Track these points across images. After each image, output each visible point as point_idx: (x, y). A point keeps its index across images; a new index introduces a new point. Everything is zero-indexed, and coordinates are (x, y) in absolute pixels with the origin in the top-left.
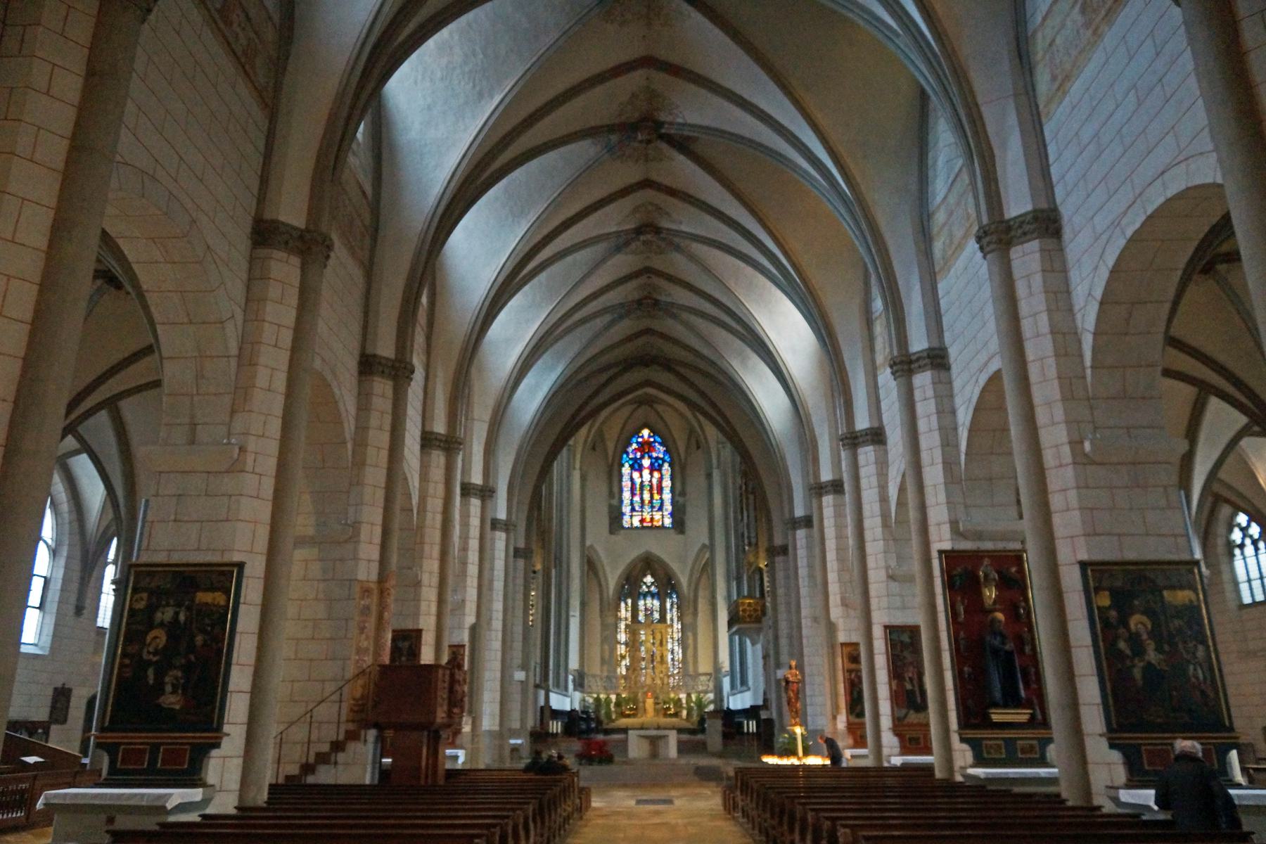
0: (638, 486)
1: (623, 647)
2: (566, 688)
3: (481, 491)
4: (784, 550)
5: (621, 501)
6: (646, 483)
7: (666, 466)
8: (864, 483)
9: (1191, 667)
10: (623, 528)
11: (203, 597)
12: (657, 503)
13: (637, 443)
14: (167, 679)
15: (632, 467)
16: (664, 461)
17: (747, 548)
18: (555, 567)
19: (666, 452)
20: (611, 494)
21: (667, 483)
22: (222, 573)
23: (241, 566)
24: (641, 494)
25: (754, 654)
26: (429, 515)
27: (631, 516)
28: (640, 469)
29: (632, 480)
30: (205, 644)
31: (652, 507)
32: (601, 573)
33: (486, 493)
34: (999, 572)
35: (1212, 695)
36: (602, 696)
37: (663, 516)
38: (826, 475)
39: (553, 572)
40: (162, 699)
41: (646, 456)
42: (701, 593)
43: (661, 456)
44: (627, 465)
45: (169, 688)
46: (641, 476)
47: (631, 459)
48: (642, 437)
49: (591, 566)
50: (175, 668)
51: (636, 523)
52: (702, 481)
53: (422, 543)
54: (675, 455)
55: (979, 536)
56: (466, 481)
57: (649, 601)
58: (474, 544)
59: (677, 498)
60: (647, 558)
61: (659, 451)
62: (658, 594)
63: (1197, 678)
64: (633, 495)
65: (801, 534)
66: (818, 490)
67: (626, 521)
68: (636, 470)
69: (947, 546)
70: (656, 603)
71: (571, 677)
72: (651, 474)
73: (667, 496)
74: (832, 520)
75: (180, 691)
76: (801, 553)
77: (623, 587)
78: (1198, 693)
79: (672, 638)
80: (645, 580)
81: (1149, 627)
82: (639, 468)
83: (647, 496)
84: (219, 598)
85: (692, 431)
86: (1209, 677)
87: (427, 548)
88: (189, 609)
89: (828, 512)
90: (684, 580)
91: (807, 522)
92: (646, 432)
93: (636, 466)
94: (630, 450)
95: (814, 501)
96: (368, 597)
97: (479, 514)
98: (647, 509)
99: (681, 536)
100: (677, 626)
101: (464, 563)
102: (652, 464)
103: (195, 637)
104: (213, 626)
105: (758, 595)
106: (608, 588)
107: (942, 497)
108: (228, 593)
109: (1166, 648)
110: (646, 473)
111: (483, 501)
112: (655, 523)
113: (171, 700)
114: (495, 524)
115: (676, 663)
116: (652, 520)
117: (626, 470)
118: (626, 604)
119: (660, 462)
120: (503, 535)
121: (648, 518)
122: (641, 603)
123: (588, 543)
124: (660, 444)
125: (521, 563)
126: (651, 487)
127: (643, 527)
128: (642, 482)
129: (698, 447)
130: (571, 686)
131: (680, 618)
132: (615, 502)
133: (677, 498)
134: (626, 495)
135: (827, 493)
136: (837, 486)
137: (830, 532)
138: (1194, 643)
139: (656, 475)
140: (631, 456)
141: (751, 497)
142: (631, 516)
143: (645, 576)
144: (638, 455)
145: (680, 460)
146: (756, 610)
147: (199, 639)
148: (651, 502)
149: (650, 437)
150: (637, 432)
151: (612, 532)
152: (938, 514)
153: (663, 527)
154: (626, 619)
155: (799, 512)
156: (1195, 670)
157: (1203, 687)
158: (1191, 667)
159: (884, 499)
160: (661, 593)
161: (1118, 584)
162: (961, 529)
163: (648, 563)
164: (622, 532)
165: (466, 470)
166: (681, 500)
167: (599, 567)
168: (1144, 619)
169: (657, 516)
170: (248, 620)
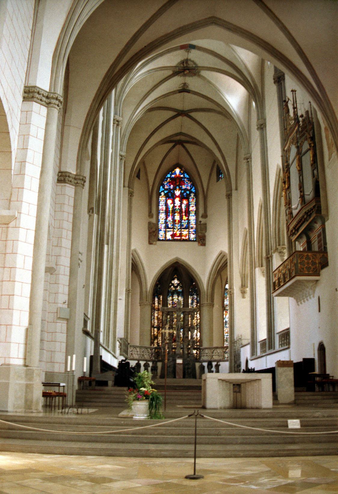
2: (114, 351)
5: (158, 221)
6: (177, 208)
7: (192, 195)
10: (159, 240)
15: (167, 196)
16: (191, 192)
18: (108, 244)
19: (193, 185)
20: (150, 215)
21: (192, 208)
24: (173, 216)
27: (165, 232)
28: (173, 197)
29: (166, 205)
31: (182, 225)
37: (189, 231)
39: (106, 247)
41: (178, 188)
43: (189, 188)
44: (163, 194)
46: (173, 203)
48: (175, 173)
51: (169, 237)
52: (225, 201)
57: (175, 297)
59: (200, 219)
62: (183, 291)
68: (169, 198)
70: (181, 299)
71: (118, 344)
73: (192, 218)
80: (173, 282)
82: (173, 197)
83: (177, 217)
92: (178, 171)
98: (178, 226)
99: (202, 247)
106: (146, 283)
110: (177, 201)
112: (183, 237)
116: (181, 235)
117: (162, 199)
118: (159, 299)
119: (188, 192)
120: (44, 110)
121: (178, 233)
122: (170, 298)
123: (133, 248)
124: (190, 180)
125: (70, 190)
128: (174, 207)
132: (154, 220)
133: (200, 219)
134: (162, 216)
139: (185, 202)
143: (174, 279)
145: (203, 191)
146: (314, 263)
148: (180, 221)
150: (171, 170)
151: (150, 243)
153: (189, 240)
164: (158, 242)
166: (203, 220)
167: (140, 266)
169: (185, 232)
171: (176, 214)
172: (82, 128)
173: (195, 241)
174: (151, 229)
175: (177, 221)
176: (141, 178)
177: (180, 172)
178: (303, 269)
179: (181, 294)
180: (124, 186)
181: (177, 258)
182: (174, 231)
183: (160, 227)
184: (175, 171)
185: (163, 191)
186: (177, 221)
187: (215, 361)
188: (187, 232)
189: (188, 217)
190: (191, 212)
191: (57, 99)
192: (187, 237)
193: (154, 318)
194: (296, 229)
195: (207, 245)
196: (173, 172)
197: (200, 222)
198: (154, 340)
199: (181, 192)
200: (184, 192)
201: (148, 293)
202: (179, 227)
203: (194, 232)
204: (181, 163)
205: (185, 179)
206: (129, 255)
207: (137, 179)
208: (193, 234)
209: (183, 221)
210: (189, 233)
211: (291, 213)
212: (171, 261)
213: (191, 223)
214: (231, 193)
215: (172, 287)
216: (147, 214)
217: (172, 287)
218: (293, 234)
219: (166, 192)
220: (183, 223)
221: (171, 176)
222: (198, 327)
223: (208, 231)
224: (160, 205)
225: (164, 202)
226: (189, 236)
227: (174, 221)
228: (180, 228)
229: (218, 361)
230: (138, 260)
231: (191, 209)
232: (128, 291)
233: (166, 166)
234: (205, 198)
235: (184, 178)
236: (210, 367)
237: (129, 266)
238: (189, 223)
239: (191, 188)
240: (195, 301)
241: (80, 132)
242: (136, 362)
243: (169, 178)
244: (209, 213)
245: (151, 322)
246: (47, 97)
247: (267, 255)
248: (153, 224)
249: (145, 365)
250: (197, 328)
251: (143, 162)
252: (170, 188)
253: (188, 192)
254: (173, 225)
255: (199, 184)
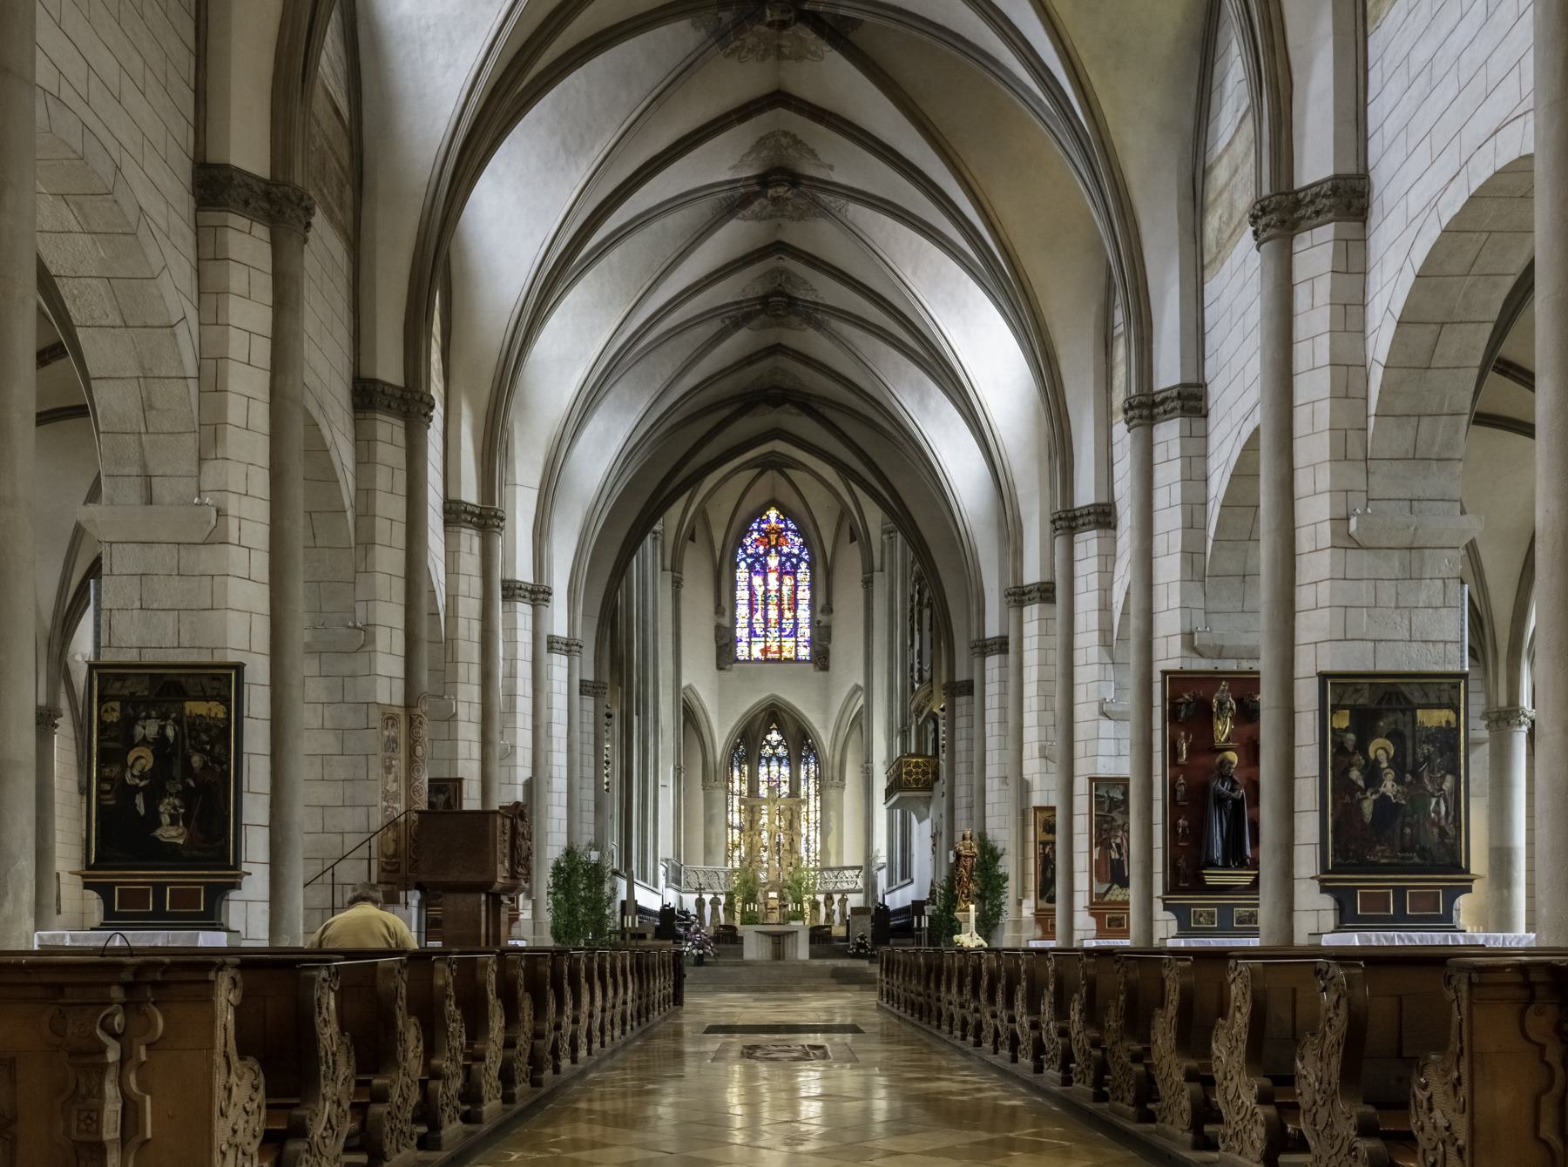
0: (759, 598)
1: (736, 832)
2: (656, 884)
3: (532, 592)
4: (968, 688)
5: (734, 620)
6: (773, 594)
7: (803, 565)
8: (1080, 585)
9: (1434, 801)
10: (737, 660)
11: (195, 708)
12: (788, 627)
13: (759, 530)
14: (162, 809)
15: (751, 567)
16: (800, 560)
17: (917, 686)
18: (638, 714)
19: (804, 544)
20: (719, 610)
21: (804, 595)
22: (215, 678)
23: (239, 668)
24: (766, 610)
25: (921, 833)
26: (462, 623)
27: (750, 643)
29: (751, 587)
30: (205, 766)
31: (782, 630)
32: (705, 730)
33: (538, 595)
34: (1239, 701)
35: (1452, 833)
36: (707, 898)
37: (797, 642)
38: (1032, 574)
39: (635, 718)
40: (158, 832)
41: (773, 550)
42: (850, 757)
43: (796, 551)
44: (743, 565)
45: (166, 819)
47: (751, 556)
48: (768, 521)
49: (690, 717)
50: (171, 795)
53: (455, 662)
54: (818, 552)
55: (1220, 653)
56: (508, 577)
58: (524, 669)
59: (819, 617)
60: (773, 705)
61: (793, 544)
63: (1438, 813)
64: (752, 610)
65: (993, 662)
66: (1018, 596)
67: (742, 650)
68: (757, 573)
69: (1174, 665)
70: (785, 771)
71: (661, 870)
72: (780, 580)
73: (804, 614)
74: (1035, 640)
75: (181, 823)
76: (992, 689)
77: (736, 748)
78: (1436, 830)
79: (807, 820)
81: (1392, 752)
83: (773, 614)
84: (217, 710)
85: (844, 513)
86: (1452, 813)
87: (462, 668)
88: (178, 722)
89: (1031, 628)
90: (824, 735)
91: (1002, 645)
92: (773, 514)
93: (758, 567)
94: (748, 541)
95: (1013, 613)
96: (393, 725)
97: (529, 626)
98: (773, 632)
99: (821, 674)
100: (814, 804)
101: (511, 696)
102: (781, 564)
103: (191, 757)
104: (212, 743)
105: (930, 753)
106: (713, 747)
107: (1176, 601)
108: (225, 701)
109: (1408, 777)
110: (772, 577)
111: (533, 606)
112: (786, 654)
113: (170, 833)
114: (553, 645)
115: (812, 855)
117: (742, 574)
118: (741, 771)
119: (794, 560)
120: (565, 659)
122: (763, 771)
123: (684, 683)
126: (780, 599)
127: (767, 660)
128: (766, 591)
129: (853, 539)
130: (662, 881)
131: (820, 792)
132: (726, 622)
133: (819, 617)
134: (742, 611)
135: (1031, 601)
136: (1046, 590)
137: (1031, 657)
138: (1443, 772)
139: (788, 580)
140: (749, 552)
141: (927, 613)
142: (750, 643)
144: (761, 550)
146: (925, 773)
147: (196, 760)
149: (779, 521)
150: (760, 512)
151: (720, 667)
152: (1169, 624)
153: (797, 660)
154: (741, 793)
155: (992, 630)
156: (1438, 803)
157: (1443, 823)
158: (1434, 801)
159: (1105, 607)
160: (793, 755)
161: (1361, 701)
162: (1196, 643)
163: (774, 714)
165: (510, 560)
168: (1388, 742)
169: (789, 644)
170: (256, 738)
171: (770, 607)
172: (598, 615)
173: (810, 661)
174: (722, 639)
175: (773, 621)
176: (697, 538)
177: (778, 517)
178: (909, 781)
179: (785, 761)
180: (663, 569)
181: (773, 695)
182: (766, 642)
183: (738, 635)
184: (768, 516)
185: (744, 559)
186: (773, 621)
187: (837, 892)
188: (794, 644)
189: (795, 611)
190: (800, 602)
191: (577, 645)
192: (793, 654)
193: (732, 811)
194: (919, 712)
195: (831, 668)
196: (764, 517)
197: (819, 622)
198: (733, 851)
199: (780, 560)
200: (786, 561)
201: (718, 766)
202: (777, 634)
203: (806, 644)
204: (781, 499)
205: (789, 533)
206: (678, 702)
207: (690, 542)
208: (805, 647)
209: (784, 621)
210: (797, 646)
211: (913, 686)
212: (761, 702)
213: (800, 625)
214: (872, 577)
215: (767, 747)
216: (713, 610)
217: (767, 747)
218: (918, 717)
219: (749, 561)
220: (784, 626)
221: (759, 526)
222: (818, 825)
223: (833, 642)
224: (739, 588)
225: (746, 583)
226: (796, 650)
227: (766, 620)
228: (780, 636)
229: (844, 893)
230: (696, 703)
231: (800, 595)
232: (678, 771)
233: (749, 505)
234: (829, 573)
235: (787, 529)
236: (829, 903)
237: (678, 711)
238: (796, 624)
239: (801, 552)
240: (813, 775)
241: (596, 621)
242: (697, 896)
243: (756, 530)
244: (835, 608)
245: (727, 819)
246: (567, 645)
247: (903, 727)
248: (725, 628)
249: (712, 902)
250: (816, 828)
251: (702, 512)
252: (756, 553)
253: (794, 560)
254: (765, 629)
255: (816, 543)
